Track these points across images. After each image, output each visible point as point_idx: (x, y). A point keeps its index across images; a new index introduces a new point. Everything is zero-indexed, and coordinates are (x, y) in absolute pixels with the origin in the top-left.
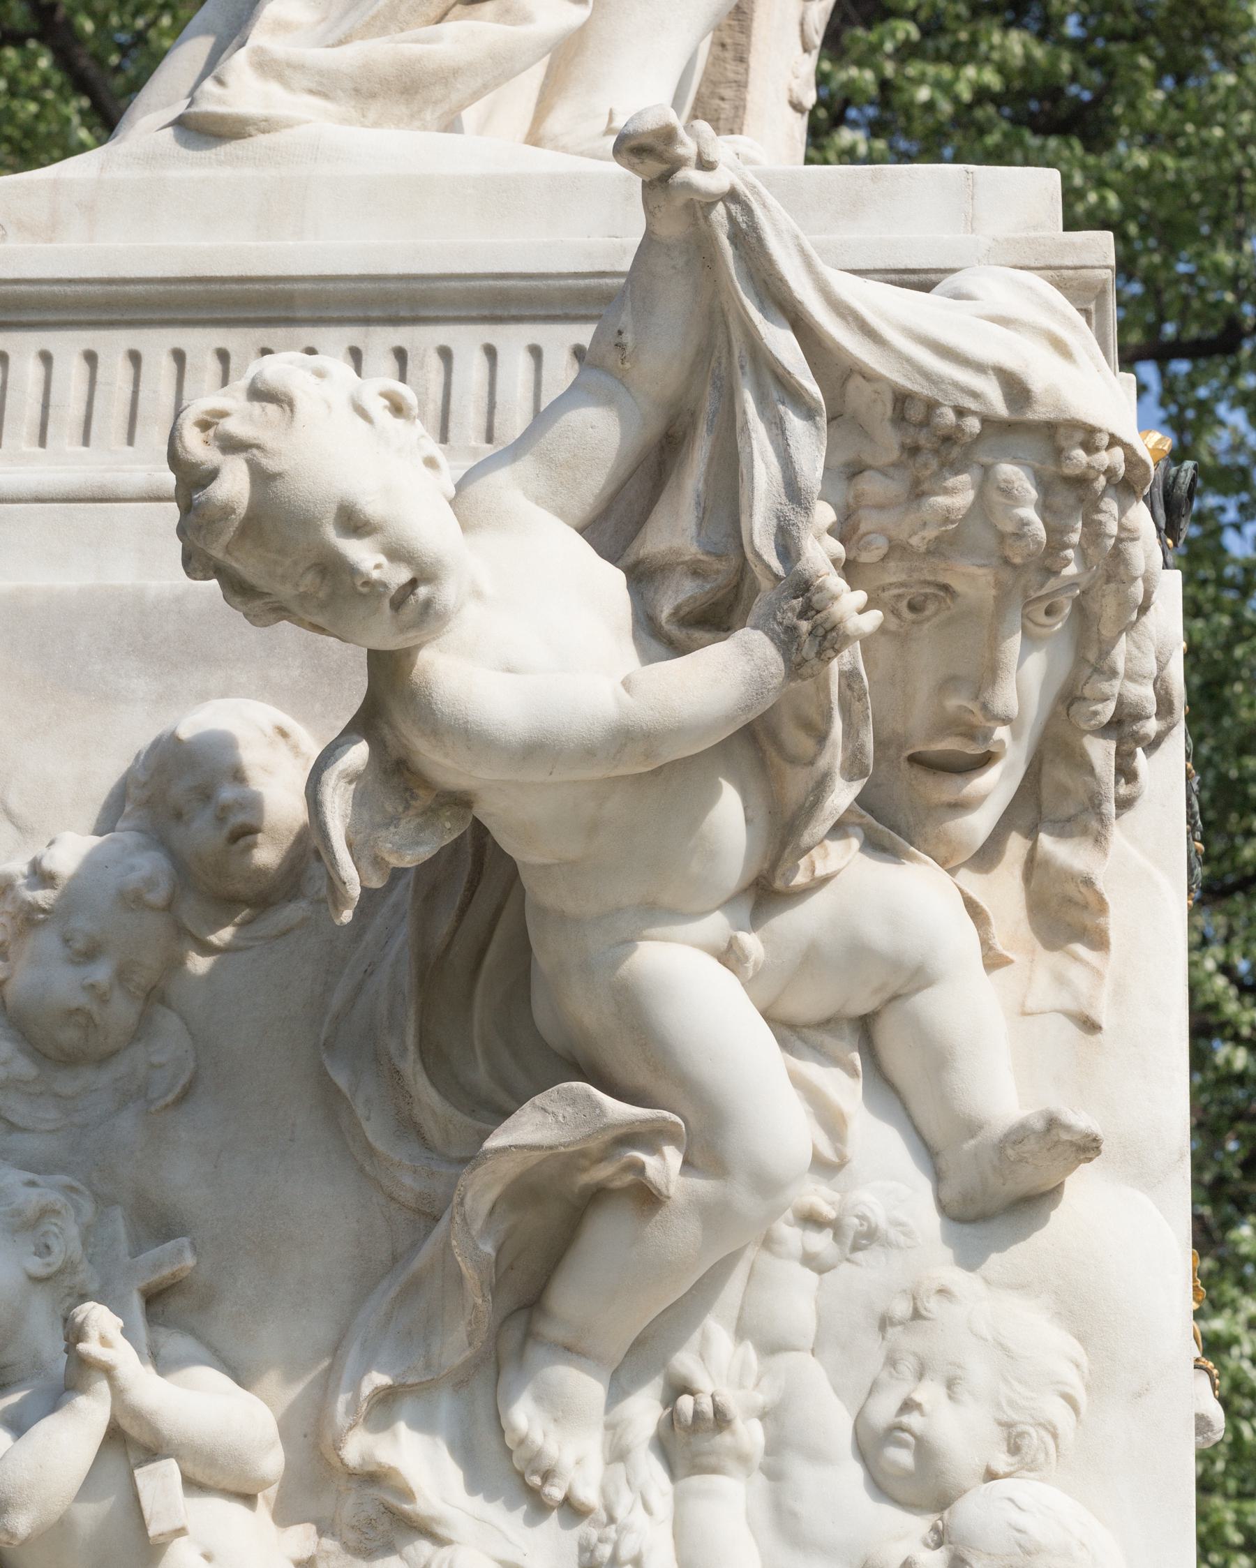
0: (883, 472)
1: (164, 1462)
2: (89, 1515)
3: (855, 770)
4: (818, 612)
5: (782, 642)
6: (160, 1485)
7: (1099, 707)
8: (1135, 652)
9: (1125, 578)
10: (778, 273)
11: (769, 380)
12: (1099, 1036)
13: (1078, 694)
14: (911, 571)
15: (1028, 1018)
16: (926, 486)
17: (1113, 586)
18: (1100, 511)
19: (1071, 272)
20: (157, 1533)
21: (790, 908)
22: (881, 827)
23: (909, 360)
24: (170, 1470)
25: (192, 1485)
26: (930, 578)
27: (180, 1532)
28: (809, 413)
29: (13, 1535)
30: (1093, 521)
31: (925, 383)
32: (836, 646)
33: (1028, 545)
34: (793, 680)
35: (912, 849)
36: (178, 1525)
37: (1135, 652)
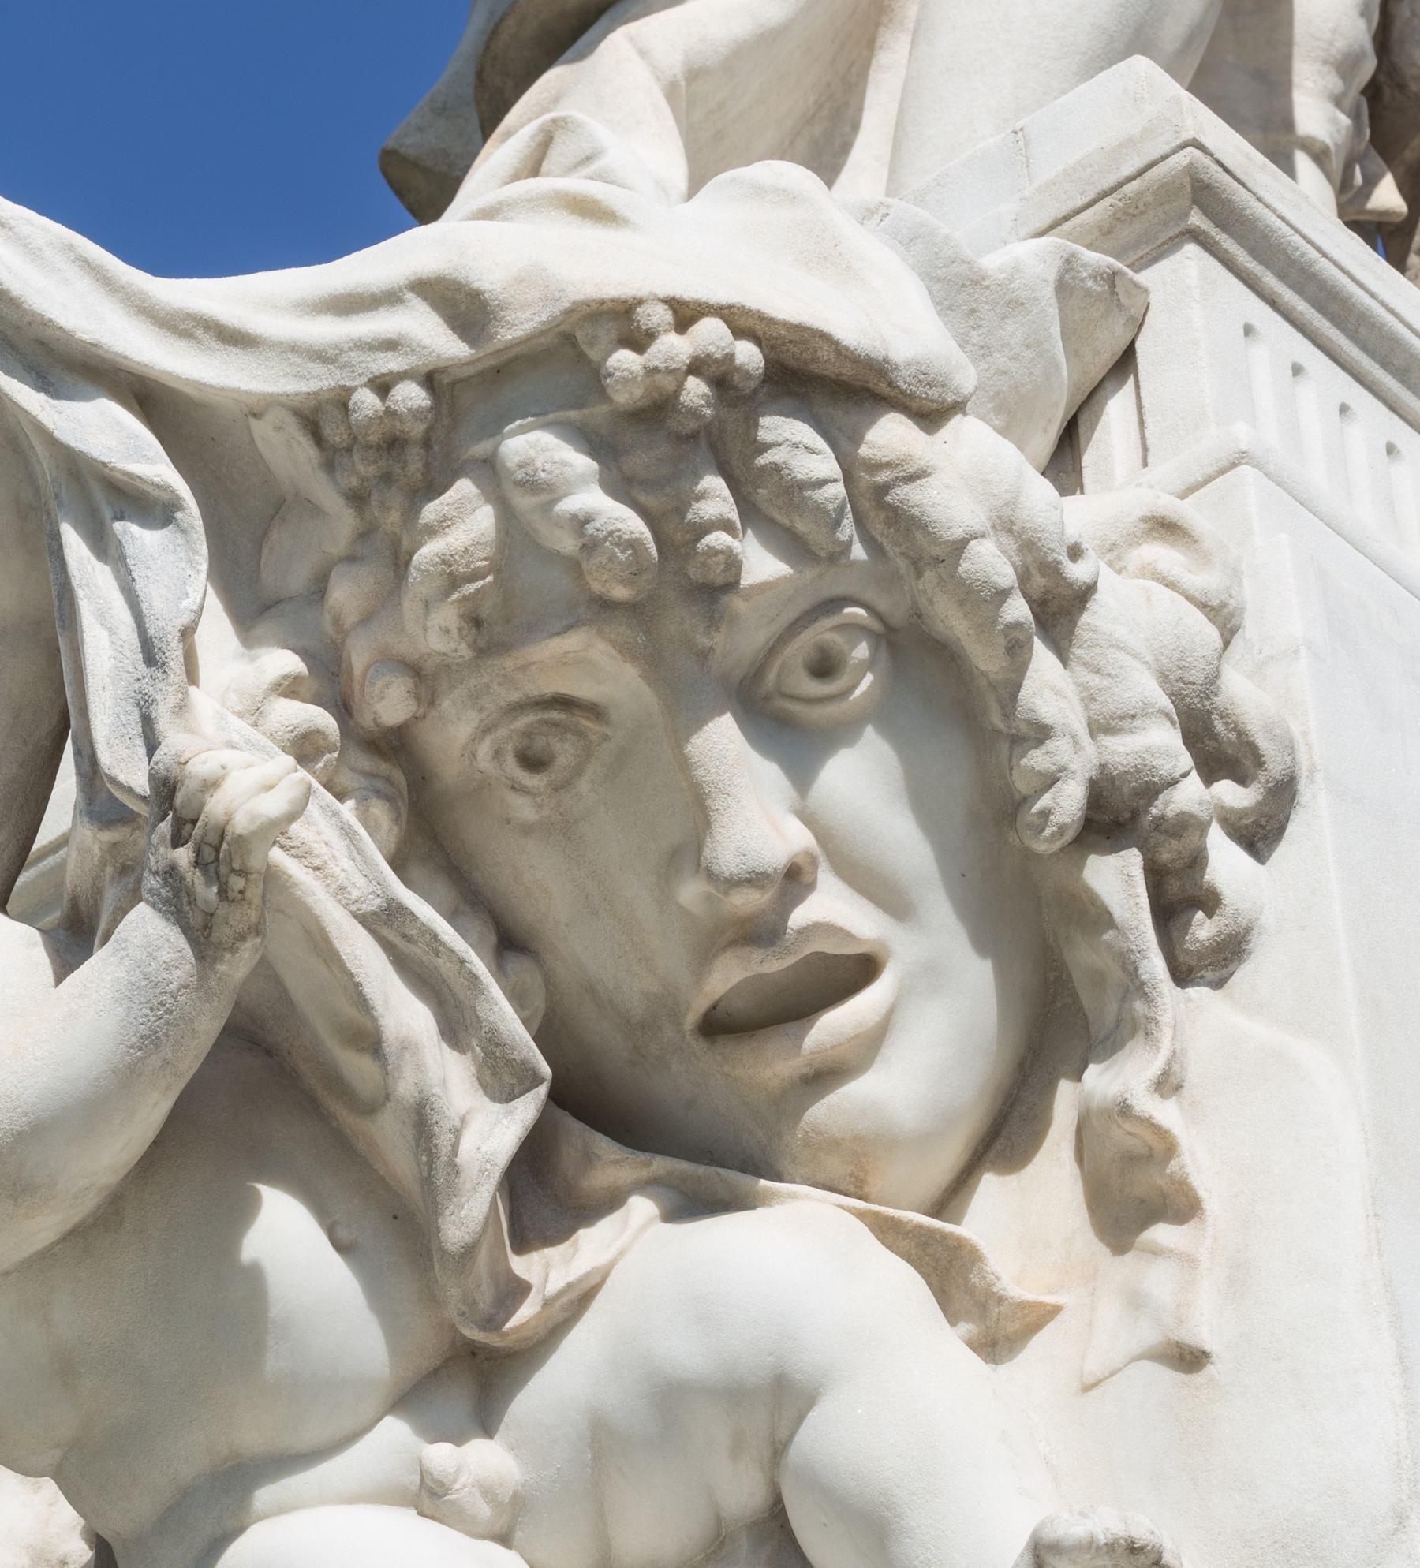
0: (351, 559)
3: (508, 1079)
4: (194, 822)
5: (167, 902)
7: (1045, 801)
8: (1095, 680)
9: (936, 551)
10: (34, 313)
11: (99, 496)
12: (1210, 1369)
13: (1017, 797)
14: (475, 698)
15: (1095, 1392)
16: (406, 543)
17: (929, 575)
18: (766, 447)
19: (1135, 184)
21: (539, 1368)
22: (701, 1170)
23: (294, 348)
26: (515, 696)
28: (155, 509)
30: (763, 469)
31: (317, 368)
32: (236, 866)
33: (612, 557)
34: (215, 960)
35: (763, 1182)
37: (1095, 680)
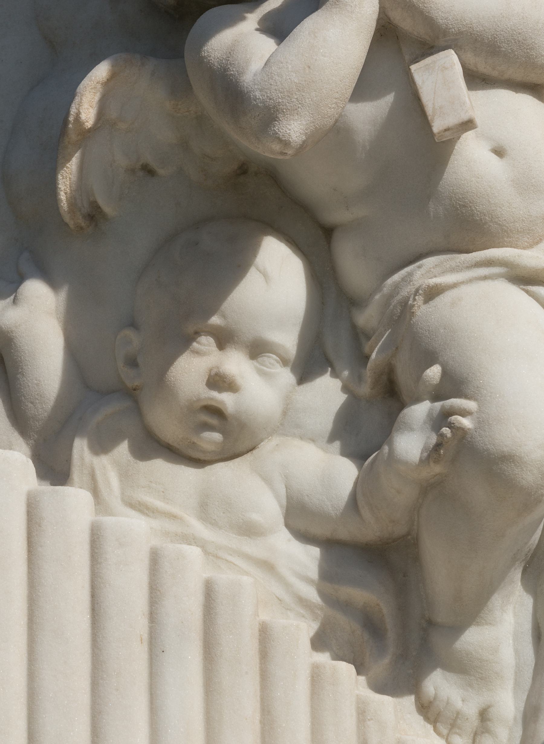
1: (442, 54)
2: (368, 116)
6: (440, 79)
20: (441, 128)
24: (450, 62)
25: (476, 79)
27: (468, 125)
29: (286, 144)
36: (464, 117)
